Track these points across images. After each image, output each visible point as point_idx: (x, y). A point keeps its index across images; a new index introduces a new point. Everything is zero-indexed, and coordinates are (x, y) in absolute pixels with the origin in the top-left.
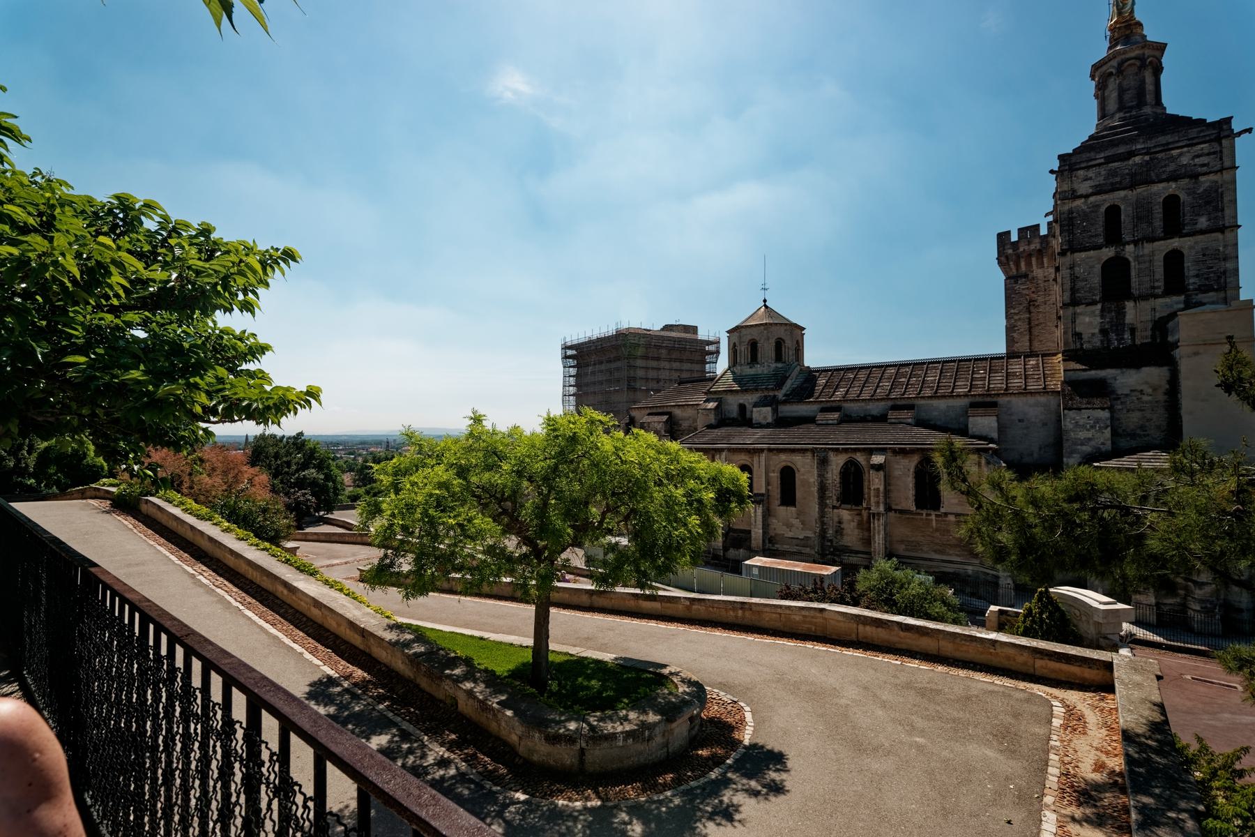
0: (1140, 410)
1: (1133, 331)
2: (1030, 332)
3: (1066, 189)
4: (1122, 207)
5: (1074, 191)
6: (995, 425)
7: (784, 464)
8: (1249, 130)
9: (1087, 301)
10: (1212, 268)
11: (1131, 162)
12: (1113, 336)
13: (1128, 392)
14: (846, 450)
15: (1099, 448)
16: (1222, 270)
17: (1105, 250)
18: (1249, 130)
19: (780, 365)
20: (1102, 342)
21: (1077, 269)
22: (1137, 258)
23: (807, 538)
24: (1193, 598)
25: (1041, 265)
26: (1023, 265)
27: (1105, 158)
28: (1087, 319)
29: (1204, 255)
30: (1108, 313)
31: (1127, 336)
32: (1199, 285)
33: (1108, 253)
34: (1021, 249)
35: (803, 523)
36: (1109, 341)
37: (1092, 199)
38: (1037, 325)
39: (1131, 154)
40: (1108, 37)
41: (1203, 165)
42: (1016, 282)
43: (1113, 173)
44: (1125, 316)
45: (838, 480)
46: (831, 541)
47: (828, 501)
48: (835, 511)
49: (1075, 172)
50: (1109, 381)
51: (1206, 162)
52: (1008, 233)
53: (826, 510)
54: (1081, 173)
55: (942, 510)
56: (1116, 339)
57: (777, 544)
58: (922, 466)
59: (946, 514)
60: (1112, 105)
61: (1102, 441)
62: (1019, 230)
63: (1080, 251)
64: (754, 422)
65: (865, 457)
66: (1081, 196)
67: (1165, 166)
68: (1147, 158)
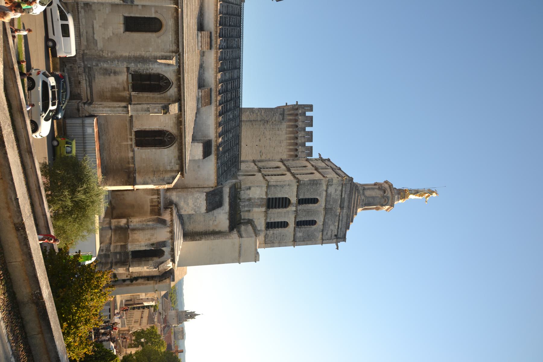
0: (204, 221)
2: (249, 121)
3: (334, 182)
4: (316, 205)
6: (197, 158)
7: (164, 22)
9: (268, 191)
10: (276, 238)
12: (247, 203)
13: (215, 215)
15: (182, 209)
16: (274, 242)
17: (296, 198)
18: (337, 248)
20: (244, 199)
21: (288, 187)
22: (288, 212)
23: (95, 43)
24: (102, 267)
25: (289, 127)
26: (291, 118)
28: (258, 192)
29: (283, 235)
30: (260, 201)
31: (246, 209)
33: (294, 200)
34: (300, 117)
35: (110, 39)
36: (244, 202)
37: (324, 193)
38: (252, 124)
39: (342, 208)
41: (327, 233)
42: (280, 114)
43: (335, 201)
44: (257, 208)
45: (153, 71)
46: (97, 65)
47: (133, 64)
48: (125, 70)
49: (341, 185)
50: (222, 207)
51: (328, 234)
52: (311, 110)
53: (125, 63)
54: (340, 188)
55: (136, 149)
56: (245, 205)
57: (85, 11)
58: (168, 135)
59: (133, 151)
60: (368, 193)
61: (187, 210)
62: (312, 117)
65: (173, 94)
66: (327, 188)
67: (331, 220)
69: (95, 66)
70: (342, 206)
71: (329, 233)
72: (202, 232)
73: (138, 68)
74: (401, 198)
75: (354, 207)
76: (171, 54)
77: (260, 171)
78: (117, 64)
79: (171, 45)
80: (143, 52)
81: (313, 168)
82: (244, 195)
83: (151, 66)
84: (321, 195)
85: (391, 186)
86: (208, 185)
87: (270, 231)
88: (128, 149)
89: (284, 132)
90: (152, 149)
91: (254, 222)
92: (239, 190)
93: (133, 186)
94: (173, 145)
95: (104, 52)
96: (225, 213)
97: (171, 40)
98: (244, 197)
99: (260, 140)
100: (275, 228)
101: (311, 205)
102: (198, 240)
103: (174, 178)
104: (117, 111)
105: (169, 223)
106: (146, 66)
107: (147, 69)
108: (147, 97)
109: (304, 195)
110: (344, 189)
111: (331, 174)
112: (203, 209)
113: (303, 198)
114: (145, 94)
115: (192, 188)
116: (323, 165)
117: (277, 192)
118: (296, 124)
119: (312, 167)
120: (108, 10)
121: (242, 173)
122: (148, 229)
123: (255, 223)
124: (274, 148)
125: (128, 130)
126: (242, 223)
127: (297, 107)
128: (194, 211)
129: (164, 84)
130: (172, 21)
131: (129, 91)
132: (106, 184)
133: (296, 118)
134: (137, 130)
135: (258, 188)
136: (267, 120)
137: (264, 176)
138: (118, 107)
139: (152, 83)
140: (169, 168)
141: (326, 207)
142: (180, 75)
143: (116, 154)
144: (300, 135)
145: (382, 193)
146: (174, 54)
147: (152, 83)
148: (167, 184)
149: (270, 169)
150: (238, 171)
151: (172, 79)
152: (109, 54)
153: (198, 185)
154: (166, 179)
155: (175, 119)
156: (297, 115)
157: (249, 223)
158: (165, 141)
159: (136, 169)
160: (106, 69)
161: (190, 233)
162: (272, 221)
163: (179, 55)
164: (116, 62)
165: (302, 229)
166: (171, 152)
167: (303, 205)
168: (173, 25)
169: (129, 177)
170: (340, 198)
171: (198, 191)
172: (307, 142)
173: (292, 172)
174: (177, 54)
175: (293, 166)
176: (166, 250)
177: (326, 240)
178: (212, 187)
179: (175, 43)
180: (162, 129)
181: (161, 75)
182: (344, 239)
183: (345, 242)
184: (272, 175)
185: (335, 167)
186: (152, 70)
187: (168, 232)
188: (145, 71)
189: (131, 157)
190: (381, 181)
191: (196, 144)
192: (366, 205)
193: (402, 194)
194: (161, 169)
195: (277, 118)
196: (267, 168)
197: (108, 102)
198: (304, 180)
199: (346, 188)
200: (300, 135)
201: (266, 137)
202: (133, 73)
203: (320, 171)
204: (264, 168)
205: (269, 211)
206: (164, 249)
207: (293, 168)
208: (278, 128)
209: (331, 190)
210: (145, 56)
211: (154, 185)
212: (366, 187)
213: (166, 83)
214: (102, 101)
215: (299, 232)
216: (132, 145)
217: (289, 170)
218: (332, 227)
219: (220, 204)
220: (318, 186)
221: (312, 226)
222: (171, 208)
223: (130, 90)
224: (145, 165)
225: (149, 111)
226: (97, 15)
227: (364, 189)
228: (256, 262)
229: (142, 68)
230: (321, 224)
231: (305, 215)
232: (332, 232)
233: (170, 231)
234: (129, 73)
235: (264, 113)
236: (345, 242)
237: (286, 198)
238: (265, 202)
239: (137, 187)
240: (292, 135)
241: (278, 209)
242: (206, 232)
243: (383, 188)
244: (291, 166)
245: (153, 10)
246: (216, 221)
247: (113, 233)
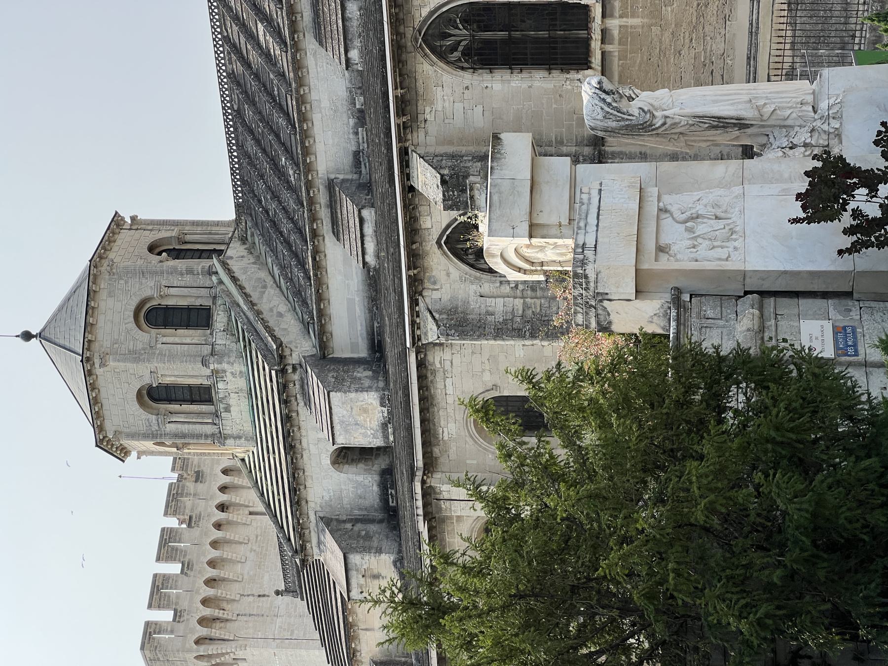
14: (415, 258)
58: (454, 48)
94: (432, 13)
130: (446, 434)
142: (409, 277)
151: (443, 259)
158: (465, 21)
168: (442, 423)
179: (434, 372)
216: (604, 16)
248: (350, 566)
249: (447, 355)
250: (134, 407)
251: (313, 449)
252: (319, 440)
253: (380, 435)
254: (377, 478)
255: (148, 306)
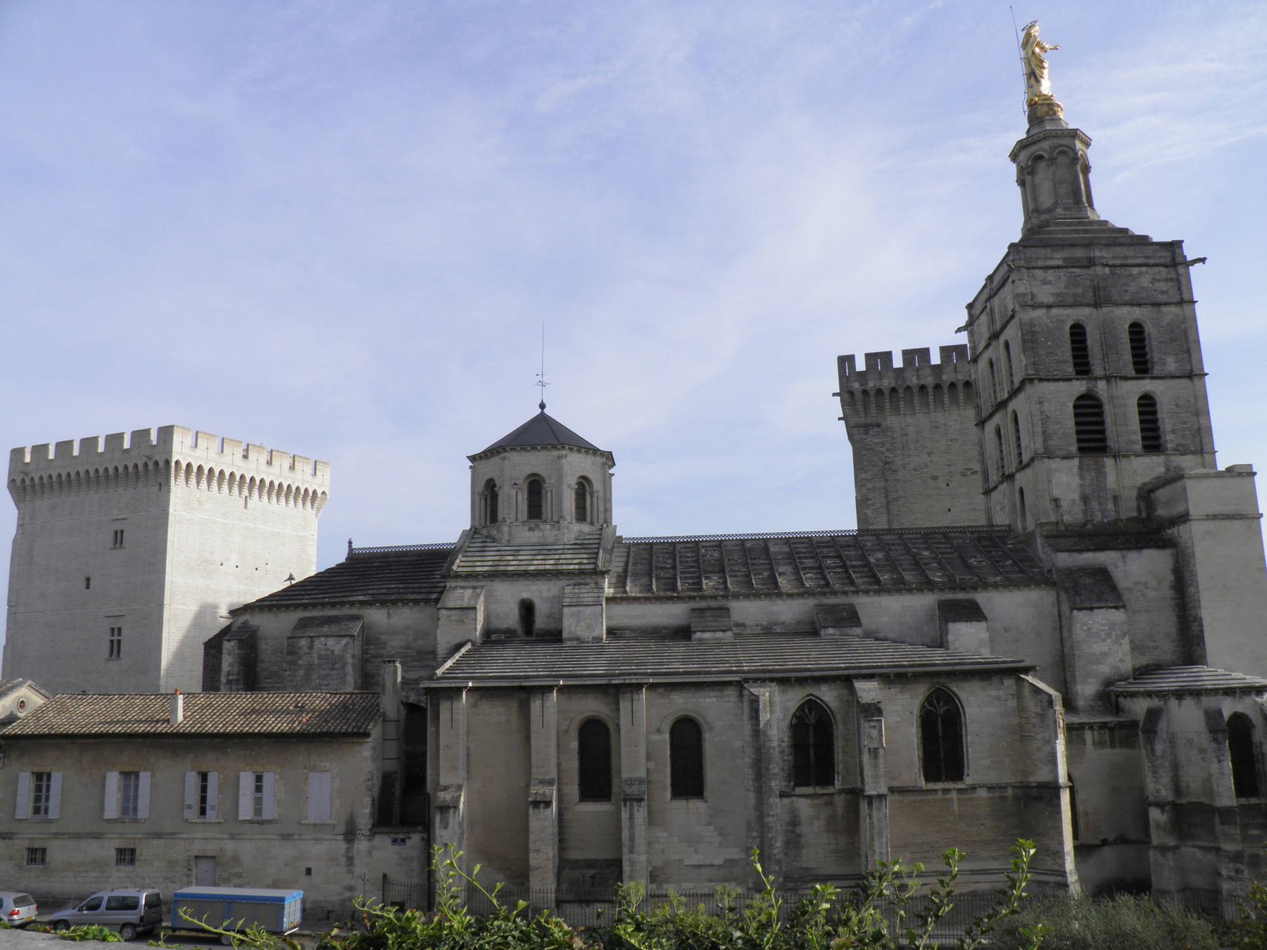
1: (1116, 498)
3: (1024, 291)
4: (1089, 329)
5: (1033, 296)
6: (985, 635)
8: (1203, 260)
10: (1185, 423)
11: (1090, 271)
12: (1095, 505)
14: (801, 681)
15: (1119, 668)
16: (1195, 427)
17: (1076, 383)
18: (1203, 260)
19: (586, 528)
20: (1085, 512)
21: (1046, 404)
25: (896, 411)
27: (1065, 260)
31: (1110, 506)
32: (1178, 445)
33: (1079, 387)
34: (871, 384)
35: (721, 832)
37: (1055, 311)
38: (896, 499)
39: (1090, 263)
40: (1027, 113)
41: (1163, 292)
42: (867, 433)
44: (1106, 478)
45: (786, 739)
46: (779, 862)
47: (773, 783)
48: (786, 801)
49: (1032, 271)
51: (1165, 289)
53: (771, 800)
54: (1039, 273)
55: (968, 781)
57: (666, 881)
58: (930, 703)
59: (973, 788)
60: (1046, 200)
61: (1121, 656)
63: (1049, 380)
64: (565, 635)
65: (835, 693)
66: (1041, 306)
67: (1127, 284)
68: (1107, 270)
69: (781, 867)
70: (1086, 263)
71: (1162, 286)
72: (1179, 617)
73: (781, 773)
74: (1051, 112)
75: (1086, 231)
76: (746, 699)
77: (1010, 477)
78: (775, 819)
79: (725, 699)
80: (746, 760)
81: (994, 343)
82: (1073, 514)
83: (775, 744)
84: (1061, 318)
85: (1022, 146)
86: (1053, 605)
87: (1166, 442)
88: (970, 800)
89: (909, 420)
90: (967, 742)
91: (1144, 484)
92: (1062, 528)
93: (1061, 790)
94: (954, 693)
95: (749, 845)
96: (1124, 561)
97: (715, 699)
98: (1081, 513)
99: (935, 478)
100: (1157, 429)
101: (1089, 342)
102: (1201, 625)
103: (1037, 691)
104: (879, 821)
105: (1155, 703)
106: (776, 754)
107: (782, 752)
108: (845, 752)
109: (1064, 362)
110: (1041, 264)
111: (1005, 298)
112: (1118, 616)
113: (1071, 364)
114: (839, 756)
115: (1062, 645)
116: (984, 319)
117: (1062, 431)
118: (887, 392)
119: (990, 348)
120: (661, 834)
121: (1019, 520)
122: (1174, 755)
123: (1147, 480)
124: (951, 440)
125: (922, 798)
126: (1148, 514)
127: (846, 395)
128: (1123, 638)
129: (813, 714)
131: (833, 794)
132: (1060, 854)
133: (872, 393)
134: (922, 777)
135: (1054, 481)
136: (882, 464)
137: (1022, 467)
138: (870, 818)
139: (811, 741)
140: (1012, 703)
141: (1092, 302)
142: (790, 678)
143: (982, 827)
144: (915, 380)
145: (1042, 166)
146: (745, 692)
147: (811, 741)
148: (1052, 708)
149: (1004, 451)
150: (1014, 530)
152: (755, 834)
153: (1055, 629)
154: (1039, 710)
155: (893, 689)
156: (865, 392)
157: (1149, 496)
158: (947, 711)
159: (1019, 780)
160: (787, 843)
161: (1184, 646)
162: (1138, 437)
163: (746, 680)
164: (770, 819)
165: (1156, 360)
166: (973, 698)
167: (1092, 363)
168: (683, 695)
169: (1039, 799)
170: (1064, 270)
171: (1070, 631)
172: (929, 360)
173: (1006, 396)
174: (746, 685)
175: (992, 395)
176: (1228, 708)
177: (1181, 293)
178: (1058, 595)
179: (721, 690)
180: (919, 720)
181: (793, 723)
182: (1175, 246)
183: (1181, 242)
184: (1019, 446)
185: (987, 291)
186: (784, 742)
187: (1179, 704)
188: (786, 758)
189: (989, 792)
190: (1012, 169)
191: (951, 638)
192: (1078, 201)
193: (1041, 111)
194: (1014, 720)
195: (877, 441)
196: (1002, 459)
197: (859, 842)
198: (1026, 366)
199: (1037, 258)
200: (915, 380)
201: (926, 464)
202: (792, 784)
203: (998, 326)
204: (1003, 467)
205: (1113, 447)
206: (1227, 714)
207: (998, 395)
208: (902, 435)
209: (1045, 295)
210: (754, 756)
211: (1056, 738)
212: (1031, 206)
213: (810, 710)
214: (859, 856)
215: (1165, 364)
216: (959, 790)
217: (1003, 405)
218: (1145, 281)
219: (1103, 575)
220: (1037, 329)
221: (1147, 332)
222: (1118, 696)
223: (830, 790)
224: (1007, 760)
225: (878, 749)
226: (672, 857)
227: (1038, 211)
228: (1255, 473)
229: (781, 762)
230: (1138, 312)
231: (1117, 353)
232: (1159, 281)
233: (1177, 699)
234: (794, 793)
235: (866, 472)
236: (1181, 242)
237: (1075, 407)
238: (1088, 461)
239: (1063, 778)
240: (917, 400)
241: (1106, 425)
242: (1178, 605)
243: (1030, 163)
244: (993, 399)
245: (655, 737)
246: (1146, 583)
247: (1190, 843)
248: (466, 611)
249: (733, 698)
250: (528, 470)
251: (534, 588)
252: (541, 592)
253: (571, 636)
254: (513, 628)
255: (586, 484)
